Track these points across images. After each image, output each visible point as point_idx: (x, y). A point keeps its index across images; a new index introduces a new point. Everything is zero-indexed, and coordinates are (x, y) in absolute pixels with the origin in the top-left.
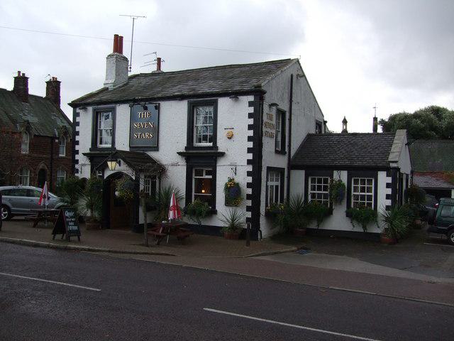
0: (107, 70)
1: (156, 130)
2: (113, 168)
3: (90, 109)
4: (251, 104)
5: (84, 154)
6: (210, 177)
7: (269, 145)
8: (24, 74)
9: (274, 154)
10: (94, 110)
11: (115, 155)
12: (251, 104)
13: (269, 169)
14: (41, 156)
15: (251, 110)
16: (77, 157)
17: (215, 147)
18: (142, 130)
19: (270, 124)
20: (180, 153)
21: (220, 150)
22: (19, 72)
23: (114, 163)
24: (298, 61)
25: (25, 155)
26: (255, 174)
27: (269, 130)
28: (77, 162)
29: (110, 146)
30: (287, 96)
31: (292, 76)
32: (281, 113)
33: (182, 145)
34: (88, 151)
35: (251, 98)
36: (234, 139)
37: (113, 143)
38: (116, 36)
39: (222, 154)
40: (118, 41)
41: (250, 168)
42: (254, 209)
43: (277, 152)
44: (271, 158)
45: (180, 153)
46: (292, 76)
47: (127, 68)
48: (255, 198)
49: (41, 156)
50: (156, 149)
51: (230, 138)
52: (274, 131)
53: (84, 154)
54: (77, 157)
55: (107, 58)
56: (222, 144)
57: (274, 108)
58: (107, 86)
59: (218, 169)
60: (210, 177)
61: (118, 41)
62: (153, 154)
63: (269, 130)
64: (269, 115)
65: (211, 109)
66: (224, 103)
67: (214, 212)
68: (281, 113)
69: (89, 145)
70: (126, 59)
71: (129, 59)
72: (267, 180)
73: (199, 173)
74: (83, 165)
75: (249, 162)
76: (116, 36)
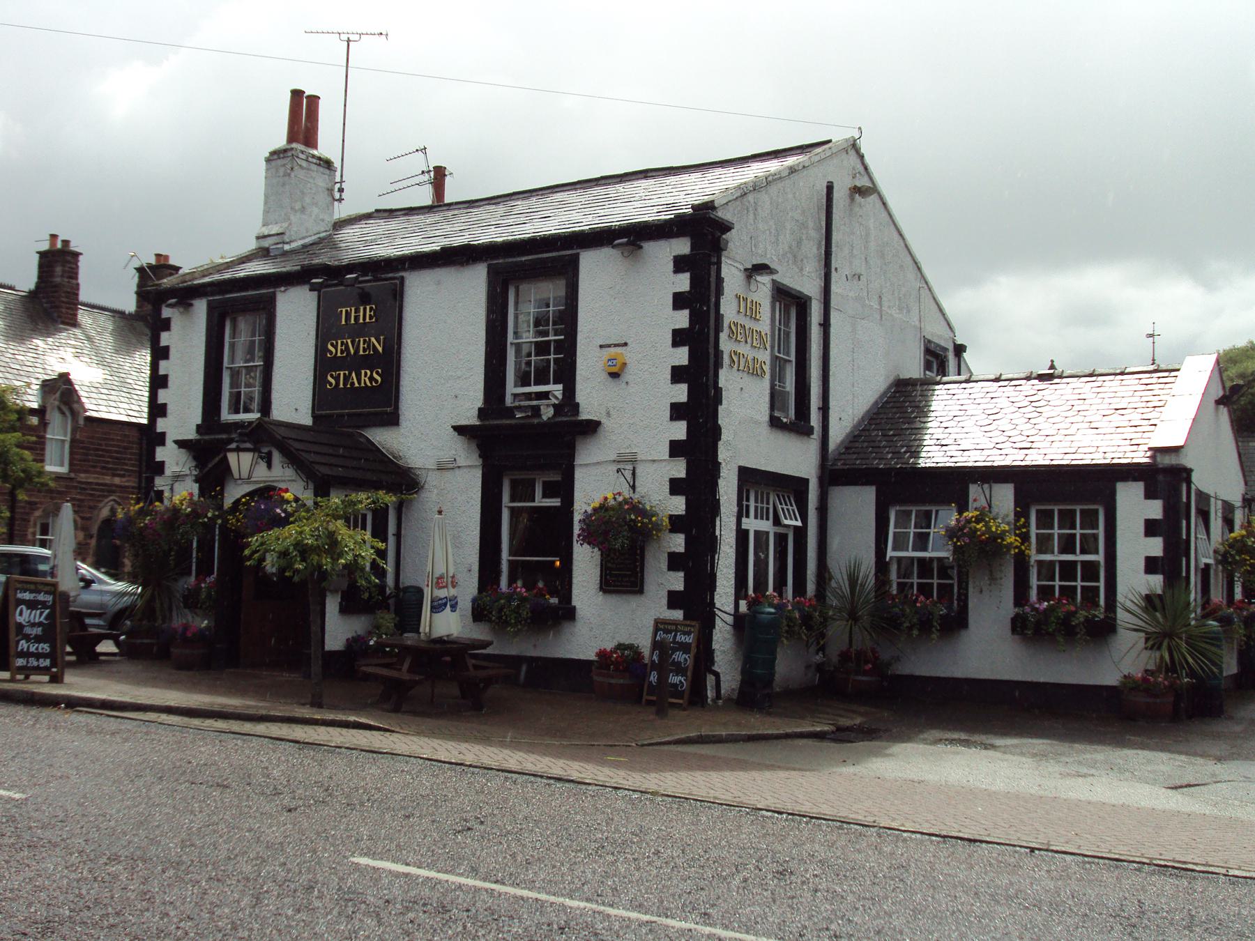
0: (266, 196)
1: (390, 362)
2: (245, 474)
3: (201, 307)
4: (680, 264)
5: (181, 444)
6: (555, 502)
7: (744, 403)
8: (66, 243)
9: (764, 429)
10: (211, 309)
11: (265, 437)
12: (680, 264)
13: (749, 477)
14: (107, 479)
15: (683, 282)
16: (161, 454)
17: (569, 402)
18: (356, 363)
19: (748, 334)
20: (460, 430)
21: (584, 416)
22: (54, 237)
23: (246, 458)
24: (854, 146)
25: (58, 478)
26: (698, 483)
27: (743, 349)
28: (160, 468)
29: (254, 416)
30: (812, 250)
31: (830, 188)
32: (790, 302)
33: (468, 401)
34: (190, 434)
35: (682, 246)
36: (627, 376)
37: (266, 407)
38: (297, 94)
39: (592, 427)
40: (304, 111)
41: (679, 469)
42: (695, 599)
43: (775, 423)
44: (748, 434)
45: (460, 430)
46: (830, 188)
47: (331, 191)
48: (696, 564)
49: (107, 479)
50: (392, 419)
51: (614, 375)
52: (765, 356)
53: (181, 444)
54: (161, 454)
55: (268, 160)
56: (592, 396)
57: (765, 279)
58: (266, 243)
59: (579, 474)
60: (555, 502)
61: (304, 111)
62: (381, 437)
63: (743, 349)
64: (744, 307)
65: (552, 290)
66: (597, 272)
67: (568, 613)
68: (790, 302)
69: (195, 415)
70: (328, 164)
71: (337, 164)
72: (742, 512)
73: (522, 491)
74: (177, 477)
75: (676, 449)
76: (297, 94)
